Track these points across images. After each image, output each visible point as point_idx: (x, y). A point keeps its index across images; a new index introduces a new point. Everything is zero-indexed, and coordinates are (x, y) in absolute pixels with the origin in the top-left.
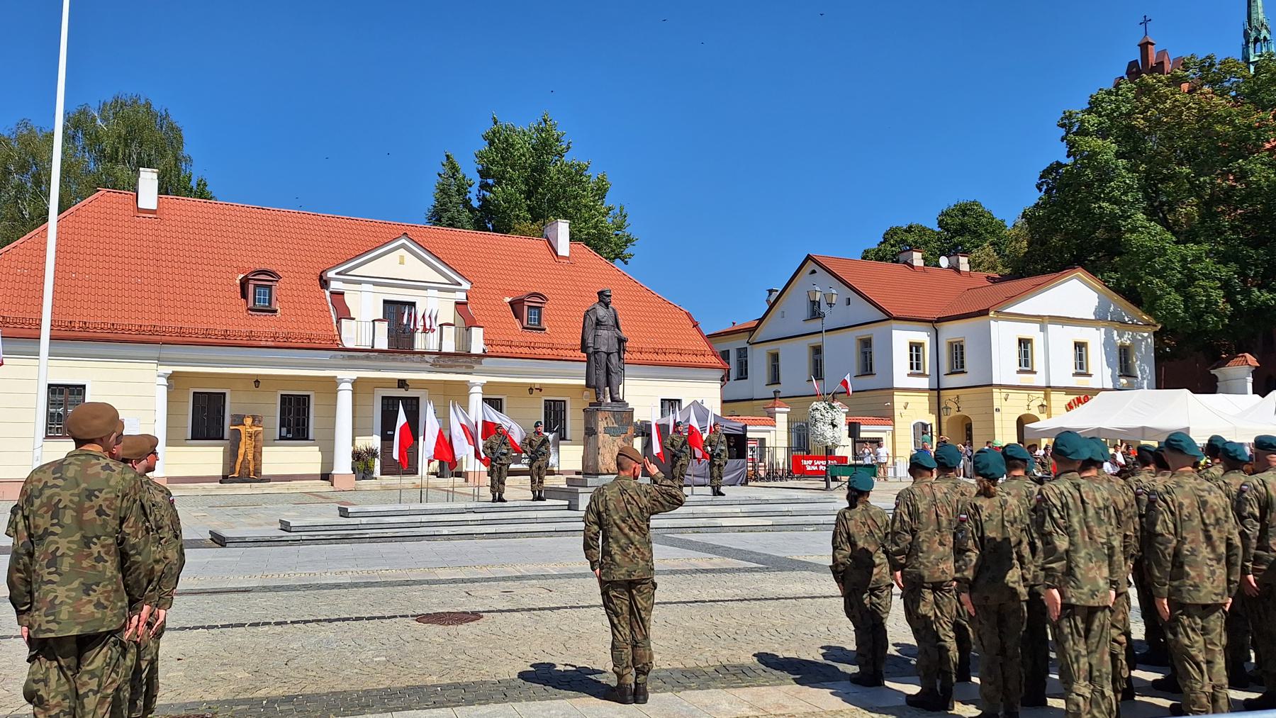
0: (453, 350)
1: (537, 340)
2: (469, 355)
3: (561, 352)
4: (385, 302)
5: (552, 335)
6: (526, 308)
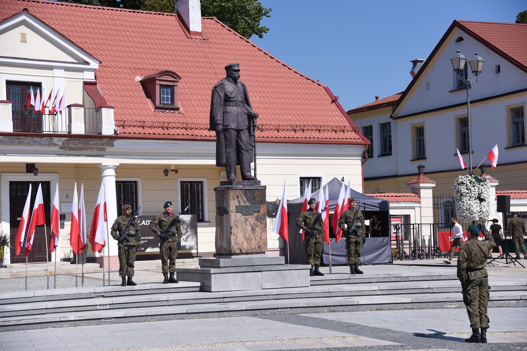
0: (82, 132)
1: (171, 120)
2: (100, 136)
3: (196, 132)
4: (9, 83)
5: (186, 114)
6: (158, 88)
